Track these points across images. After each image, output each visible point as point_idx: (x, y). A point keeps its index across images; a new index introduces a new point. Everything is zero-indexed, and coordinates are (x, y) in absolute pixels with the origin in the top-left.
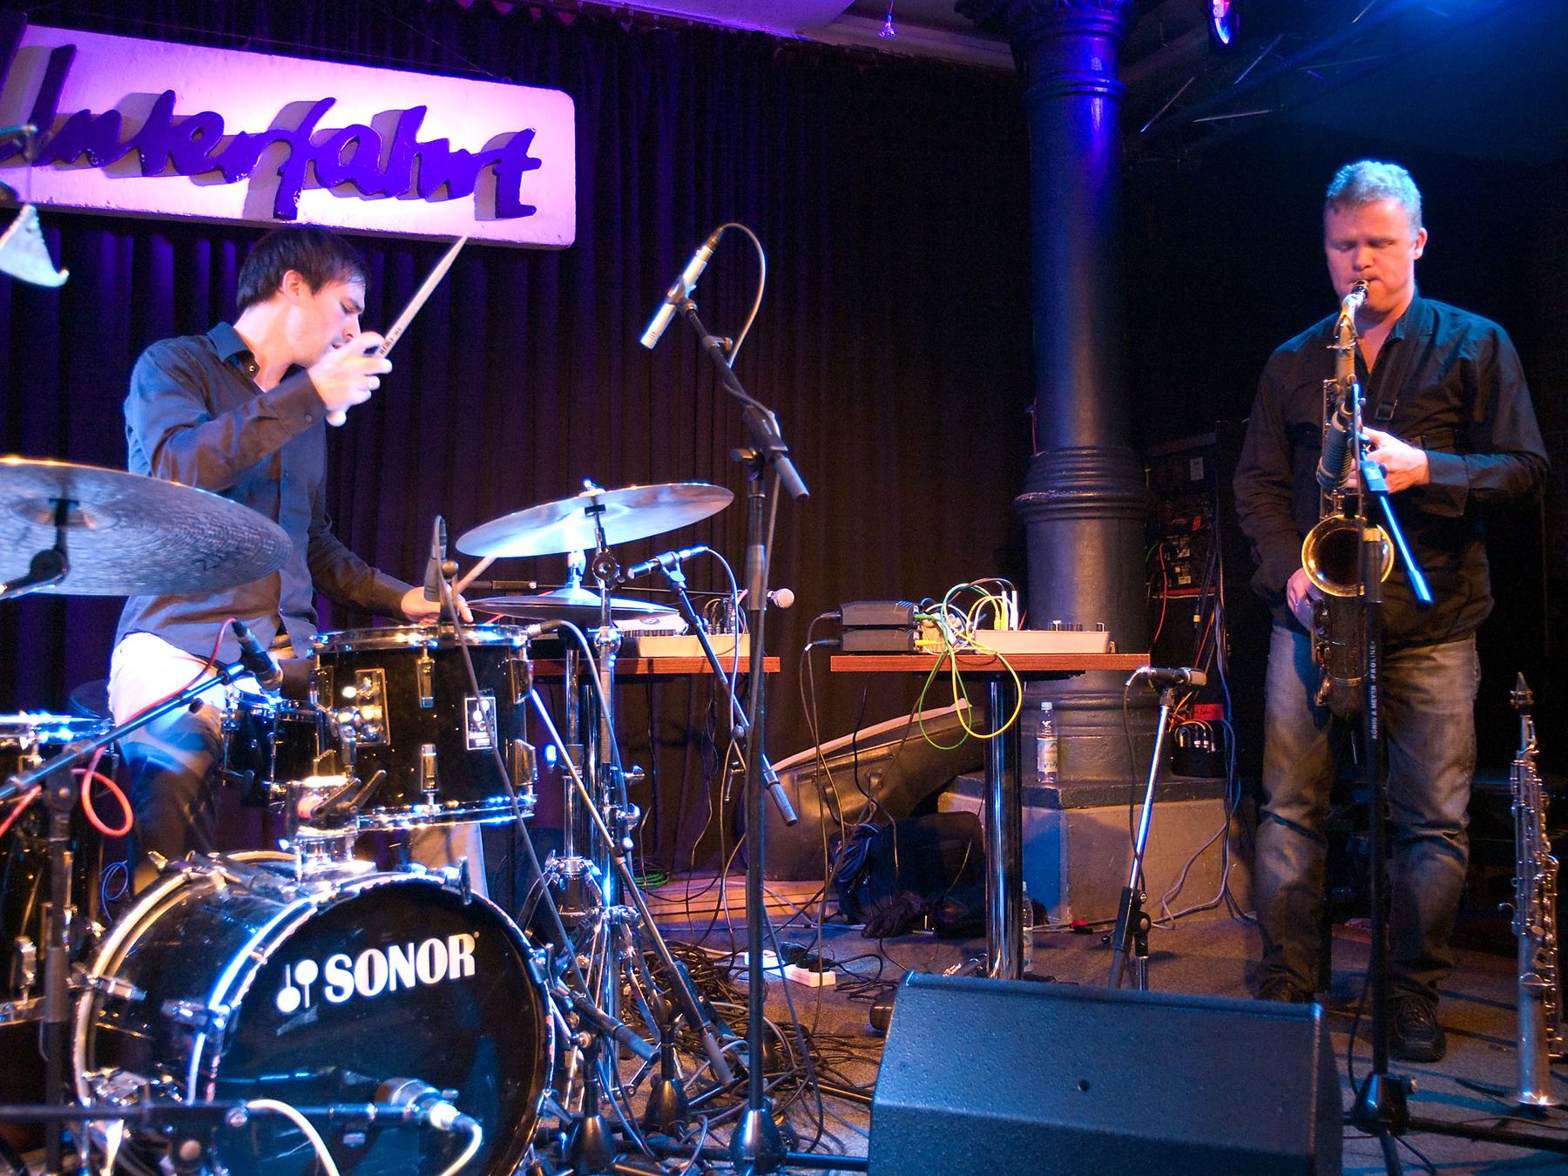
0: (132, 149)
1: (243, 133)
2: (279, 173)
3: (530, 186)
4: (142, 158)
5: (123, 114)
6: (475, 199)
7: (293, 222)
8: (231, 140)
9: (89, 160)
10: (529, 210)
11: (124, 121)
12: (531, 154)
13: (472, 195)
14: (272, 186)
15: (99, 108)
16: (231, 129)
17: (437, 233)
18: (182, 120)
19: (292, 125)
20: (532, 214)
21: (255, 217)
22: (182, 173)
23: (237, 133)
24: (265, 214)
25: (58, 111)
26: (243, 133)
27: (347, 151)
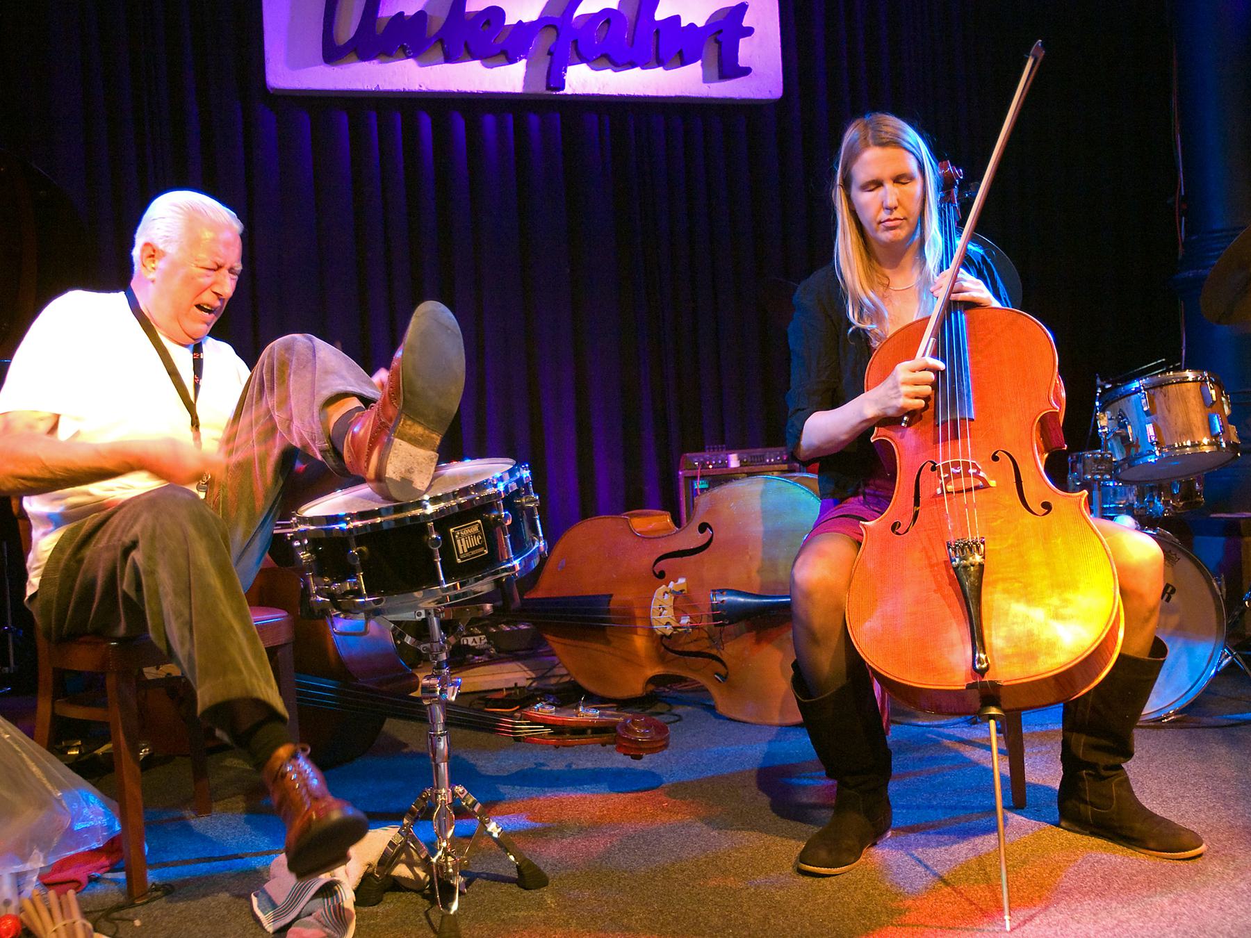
0: (436, 42)
1: (520, 22)
2: (550, 53)
3: (746, 50)
4: (443, 48)
6: (702, 65)
7: (561, 92)
8: (510, 30)
9: (404, 51)
10: (746, 71)
11: (428, 17)
12: (746, 23)
13: (700, 62)
14: (544, 63)
15: (410, 11)
16: (510, 20)
17: (673, 95)
19: (557, 13)
21: (531, 90)
22: (474, 59)
23: (515, 22)
24: (540, 88)
25: (379, 15)
26: (520, 22)
27: (601, 31)
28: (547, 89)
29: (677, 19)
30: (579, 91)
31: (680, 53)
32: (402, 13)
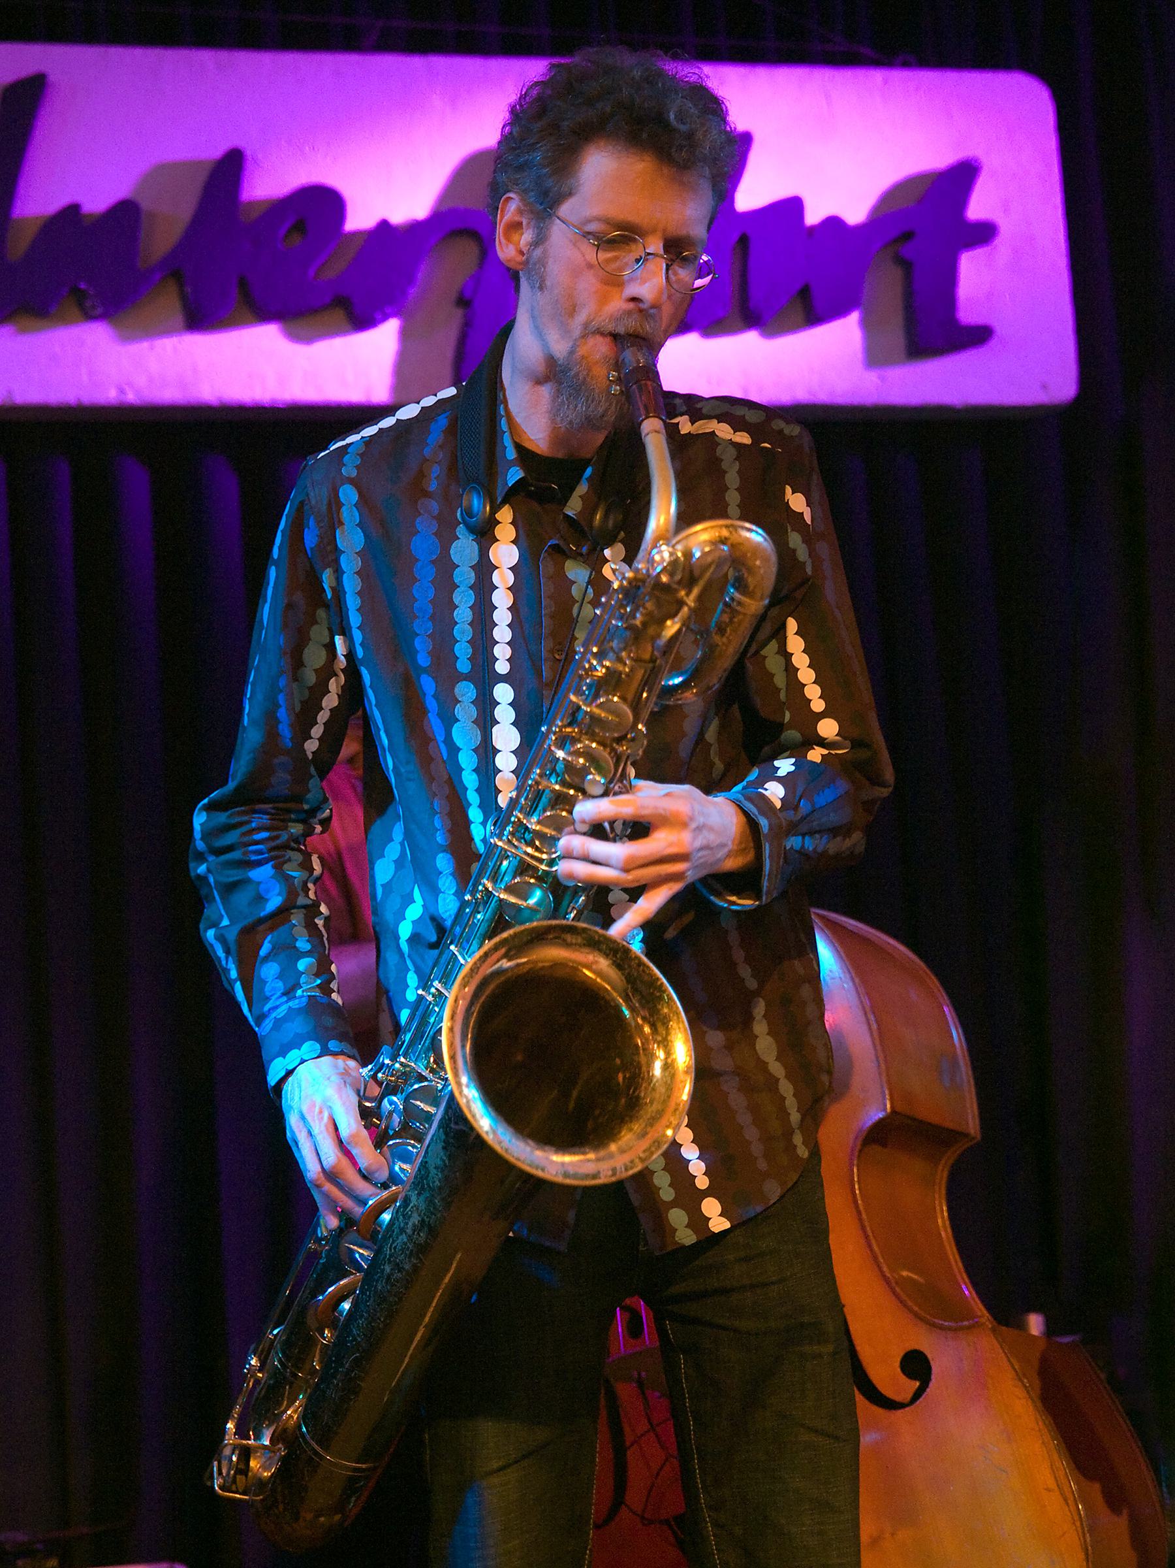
2: (463, 301)
5: (145, 205)
8: (360, 242)
10: (979, 336)
13: (854, 317)
15: (96, 203)
16: (359, 219)
25: (14, 216)
29: (792, 207)
31: (805, 293)
32: (73, 210)
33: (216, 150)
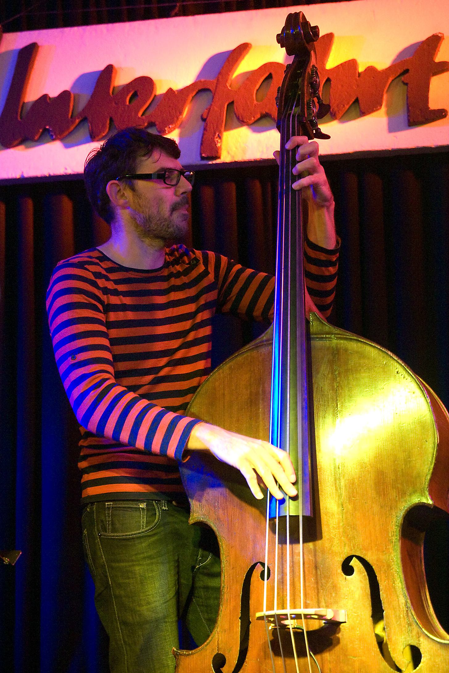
1: (170, 90)
2: (204, 120)
7: (218, 161)
15: (54, 93)
16: (161, 90)
18: (121, 88)
20: (445, 116)
26: (170, 90)
28: (203, 158)
29: (352, 64)
30: (239, 158)
33: (101, 67)
